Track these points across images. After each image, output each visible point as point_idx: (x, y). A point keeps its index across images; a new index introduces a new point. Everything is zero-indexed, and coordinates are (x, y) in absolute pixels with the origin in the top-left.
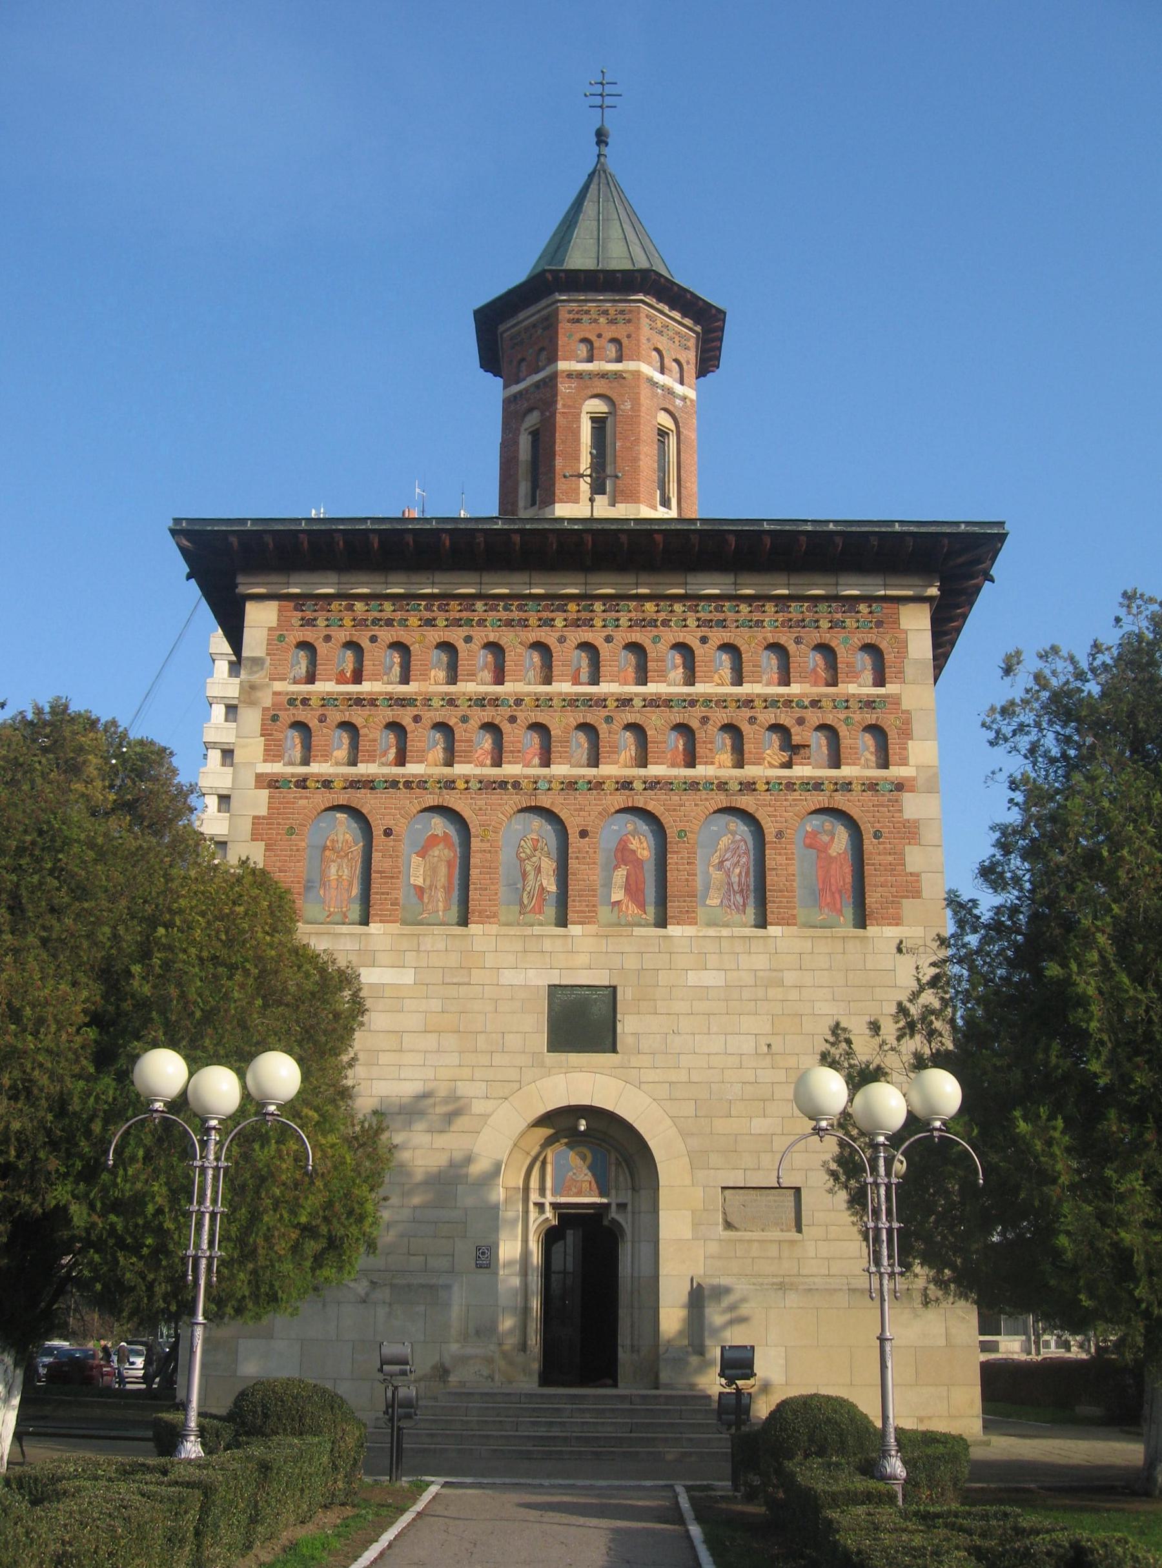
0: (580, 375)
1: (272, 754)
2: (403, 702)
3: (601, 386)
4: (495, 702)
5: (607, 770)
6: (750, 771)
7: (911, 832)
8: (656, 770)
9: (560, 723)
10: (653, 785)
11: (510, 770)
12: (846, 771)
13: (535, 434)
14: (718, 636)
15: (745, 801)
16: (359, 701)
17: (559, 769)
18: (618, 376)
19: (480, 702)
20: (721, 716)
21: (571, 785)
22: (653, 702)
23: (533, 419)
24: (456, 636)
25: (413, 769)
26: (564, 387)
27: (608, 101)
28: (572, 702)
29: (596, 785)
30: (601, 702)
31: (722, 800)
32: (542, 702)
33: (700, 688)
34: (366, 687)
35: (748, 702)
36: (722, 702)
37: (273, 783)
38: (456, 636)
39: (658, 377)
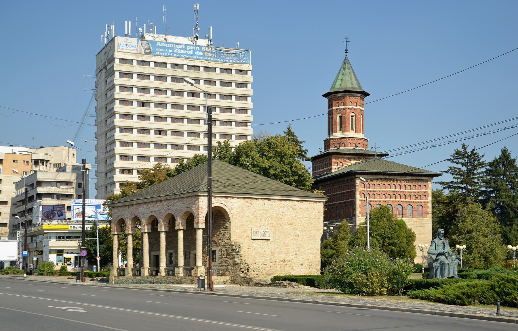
0: (350, 108)
1: (361, 197)
2: (375, 191)
3: (353, 111)
4: (385, 191)
5: (397, 200)
6: (412, 200)
7: (428, 207)
8: (402, 200)
9: (391, 194)
10: (401, 202)
11: (386, 200)
12: (422, 200)
13: (341, 117)
14: (409, 184)
15: (411, 204)
16: (370, 191)
17: (392, 200)
18: (356, 109)
19: (383, 191)
20: (409, 194)
21: (393, 201)
22: (401, 192)
23: (340, 115)
24: (380, 183)
25: (376, 199)
26: (348, 111)
27: (345, 43)
28: (393, 191)
29: (395, 201)
30: (396, 192)
31: (409, 204)
32: (390, 191)
33: (406, 190)
34: (370, 189)
35: (411, 192)
36: (409, 192)
37: (361, 201)
38: (380, 183)
39: (361, 108)
